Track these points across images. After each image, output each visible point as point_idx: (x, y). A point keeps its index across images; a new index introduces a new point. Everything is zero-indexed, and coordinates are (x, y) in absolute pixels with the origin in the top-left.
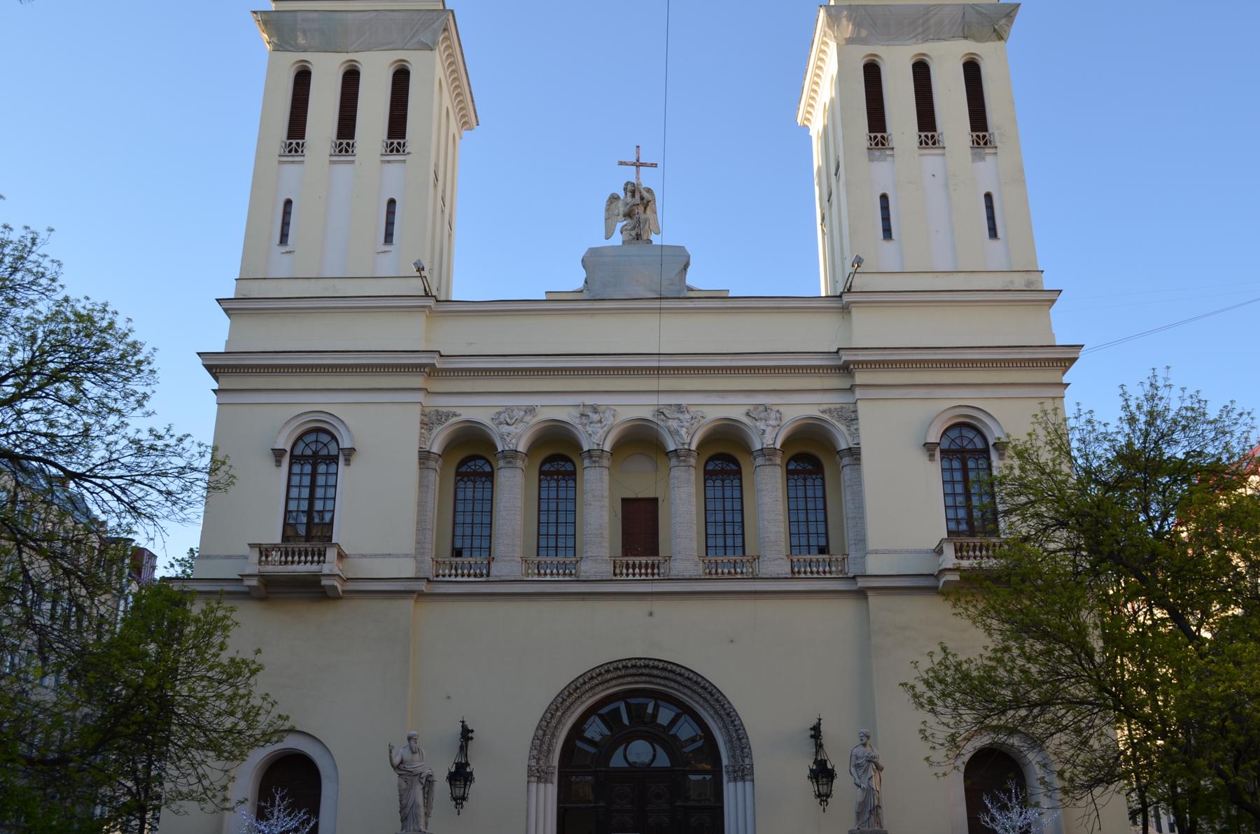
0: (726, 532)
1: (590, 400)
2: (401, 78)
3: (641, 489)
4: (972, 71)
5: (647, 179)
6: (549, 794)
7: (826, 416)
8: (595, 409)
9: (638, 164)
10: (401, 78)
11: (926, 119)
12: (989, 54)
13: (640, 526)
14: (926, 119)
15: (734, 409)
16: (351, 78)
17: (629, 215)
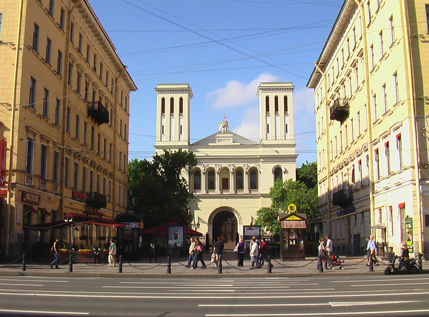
0: (239, 185)
1: (217, 164)
2: (181, 100)
3: (225, 177)
4: (286, 98)
5: (226, 119)
6: (211, 226)
7: (256, 166)
8: (218, 165)
9: (225, 117)
10: (181, 100)
11: (277, 109)
12: (289, 95)
13: (225, 185)
14: (277, 109)
15: (241, 165)
16: (172, 100)
17: (224, 127)
